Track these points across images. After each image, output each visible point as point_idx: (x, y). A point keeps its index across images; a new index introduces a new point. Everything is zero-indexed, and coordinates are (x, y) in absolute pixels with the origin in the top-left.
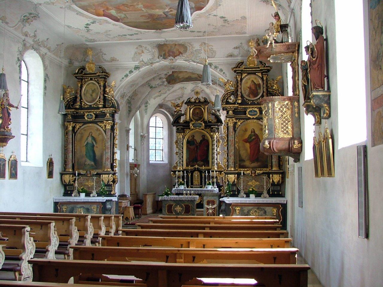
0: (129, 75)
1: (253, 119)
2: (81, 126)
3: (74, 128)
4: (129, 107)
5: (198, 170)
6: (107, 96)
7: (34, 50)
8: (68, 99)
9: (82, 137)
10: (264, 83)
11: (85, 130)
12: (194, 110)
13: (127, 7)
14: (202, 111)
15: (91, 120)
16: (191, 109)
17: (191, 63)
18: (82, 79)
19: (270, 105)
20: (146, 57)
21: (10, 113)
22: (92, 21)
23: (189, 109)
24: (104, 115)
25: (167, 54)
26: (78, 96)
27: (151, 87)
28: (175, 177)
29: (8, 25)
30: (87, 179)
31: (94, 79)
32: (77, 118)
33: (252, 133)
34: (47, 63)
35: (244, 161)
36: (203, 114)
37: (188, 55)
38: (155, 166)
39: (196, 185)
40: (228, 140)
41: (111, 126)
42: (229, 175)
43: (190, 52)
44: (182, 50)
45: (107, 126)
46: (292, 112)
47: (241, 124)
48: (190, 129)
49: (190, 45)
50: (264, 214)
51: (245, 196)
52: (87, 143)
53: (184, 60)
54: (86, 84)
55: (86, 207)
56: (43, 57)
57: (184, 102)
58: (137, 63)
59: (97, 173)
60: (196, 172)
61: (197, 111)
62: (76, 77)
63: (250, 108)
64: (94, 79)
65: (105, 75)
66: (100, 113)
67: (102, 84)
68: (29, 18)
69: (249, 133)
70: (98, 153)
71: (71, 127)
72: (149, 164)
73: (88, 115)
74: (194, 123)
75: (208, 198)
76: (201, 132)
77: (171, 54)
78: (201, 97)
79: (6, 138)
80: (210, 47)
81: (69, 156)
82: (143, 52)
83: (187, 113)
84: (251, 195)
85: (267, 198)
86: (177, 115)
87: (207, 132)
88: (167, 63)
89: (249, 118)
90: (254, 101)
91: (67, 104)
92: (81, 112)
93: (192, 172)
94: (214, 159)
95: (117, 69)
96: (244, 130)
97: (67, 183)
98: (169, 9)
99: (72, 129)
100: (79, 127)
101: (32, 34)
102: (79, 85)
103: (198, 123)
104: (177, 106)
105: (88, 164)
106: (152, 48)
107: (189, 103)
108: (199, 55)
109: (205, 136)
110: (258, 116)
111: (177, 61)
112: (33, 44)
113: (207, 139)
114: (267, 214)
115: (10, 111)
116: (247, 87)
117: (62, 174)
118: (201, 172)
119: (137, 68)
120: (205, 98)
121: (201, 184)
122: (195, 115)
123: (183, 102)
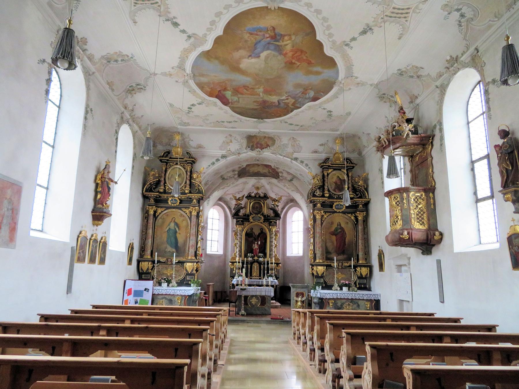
0: (216, 163)
1: (339, 212)
2: (163, 210)
3: (155, 212)
6: (194, 182)
7: (129, 125)
8: (151, 182)
9: (163, 223)
10: (349, 179)
11: (167, 215)
12: (254, 204)
13: (246, 90)
14: (261, 205)
15: (175, 205)
17: (278, 156)
18: (167, 163)
19: (405, 195)
20: (234, 147)
21: (110, 188)
22: (200, 101)
23: (249, 203)
24: (190, 200)
25: (255, 146)
26: (162, 179)
29: (114, 92)
30: (166, 267)
31: (180, 164)
32: (158, 201)
33: (338, 226)
34: (136, 142)
35: (330, 253)
36: (262, 209)
37: (275, 148)
38: (211, 256)
39: (255, 277)
40: (314, 233)
41: (197, 212)
42: (318, 267)
43: (278, 146)
44: (270, 143)
45: (193, 212)
46: (427, 203)
47: (327, 217)
48: (249, 221)
49: (279, 139)
50: (358, 308)
51: (339, 289)
52: (169, 229)
53: (271, 153)
54: (171, 169)
55: (168, 299)
56: (134, 134)
58: (224, 152)
59: (179, 261)
60: (256, 263)
61: (257, 205)
62: (161, 160)
63: (336, 202)
64: (180, 164)
65: (193, 161)
66: (185, 199)
67: (189, 170)
68: (133, 90)
69: (335, 226)
70: (181, 240)
71: (152, 211)
72: (207, 255)
73: (172, 200)
74: (254, 217)
75: (297, 290)
77: (259, 146)
78: (261, 192)
79: (104, 215)
80: (297, 142)
81: (148, 242)
82: (231, 142)
83: (248, 207)
84: (344, 288)
85: (339, 291)
88: (254, 154)
89: (336, 212)
90: (340, 196)
91: (149, 187)
92: (164, 196)
93: (252, 263)
94: (272, 252)
95: (203, 156)
96: (331, 223)
97: (145, 271)
98: (286, 97)
99: (154, 213)
100: (161, 212)
101: (131, 108)
102: (164, 169)
104: (238, 199)
105: (168, 250)
106: (241, 138)
107: (249, 197)
108: (286, 149)
110: (344, 210)
111: (264, 153)
112: (129, 119)
114: (361, 307)
115: (110, 186)
116: (333, 182)
117: (139, 262)
118: (260, 263)
119: (224, 157)
121: (260, 276)
123: (243, 196)
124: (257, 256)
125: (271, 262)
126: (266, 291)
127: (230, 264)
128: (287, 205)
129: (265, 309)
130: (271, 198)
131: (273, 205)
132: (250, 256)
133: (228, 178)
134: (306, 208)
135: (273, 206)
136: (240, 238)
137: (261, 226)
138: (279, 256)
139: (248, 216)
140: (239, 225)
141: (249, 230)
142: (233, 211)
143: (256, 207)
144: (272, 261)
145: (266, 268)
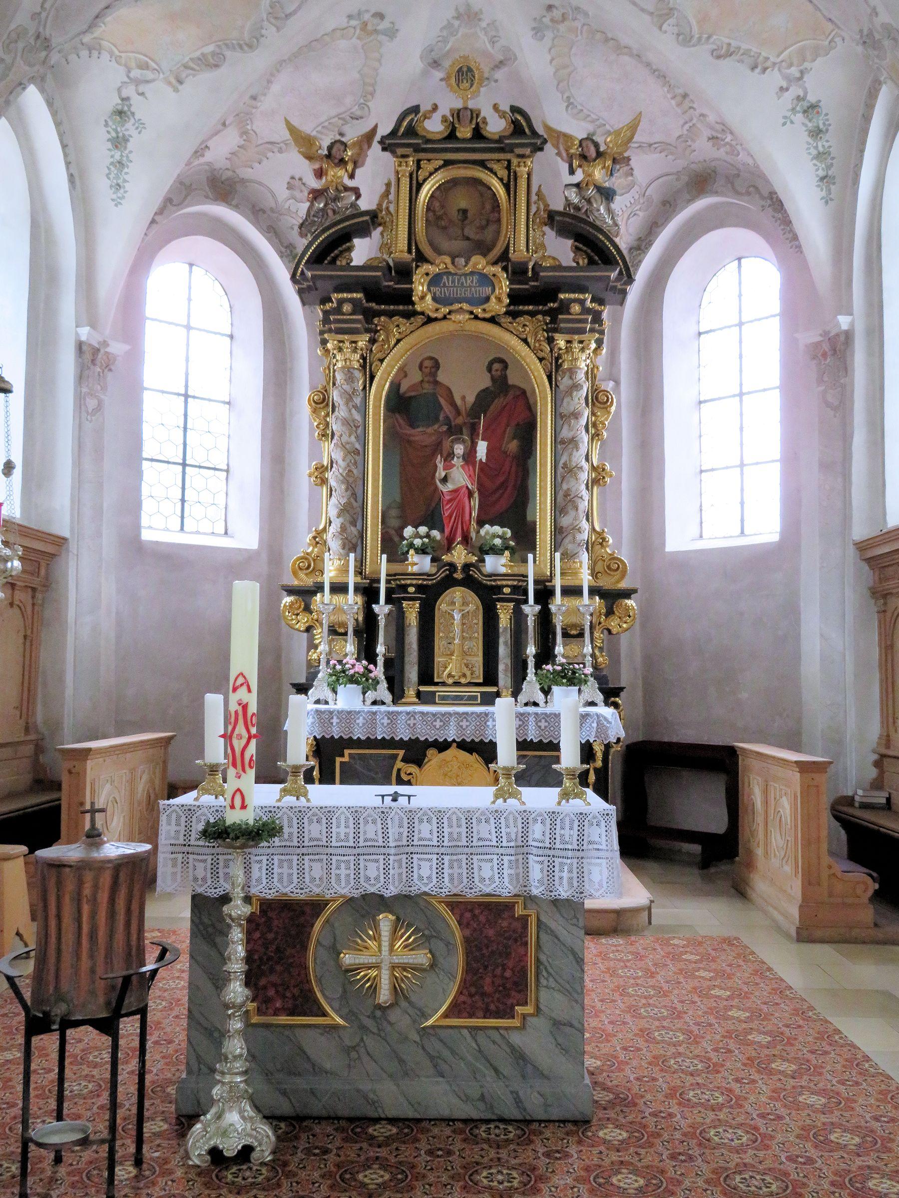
5: (470, 581)
12: (444, 189)
16: (419, 186)
28: (308, 629)
39: (457, 684)
57: (378, 138)
60: (458, 593)
61: (461, 200)
76: (478, 338)
86: (332, 218)
87: (525, 341)
94: (572, 513)
103: (468, 269)
104: (329, 156)
109: (506, 366)
113: (522, 386)
120: (515, 109)
121: (490, 678)
122: (445, 228)
123: (369, 137)
124: (466, 540)
125: (571, 582)
126: (522, 848)
127: (288, 600)
128: (667, 220)
129: (519, 1057)
131: (577, 185)
132: (418, 542)
135: (576, 200)
136: (346, 422)
137: (499, 347)
138: (618, 544)
140: (339, 331)
141: (416, 376)
142: (301, 243)
143: (454, 214)
144: (576, 573)
145: (531, 622)
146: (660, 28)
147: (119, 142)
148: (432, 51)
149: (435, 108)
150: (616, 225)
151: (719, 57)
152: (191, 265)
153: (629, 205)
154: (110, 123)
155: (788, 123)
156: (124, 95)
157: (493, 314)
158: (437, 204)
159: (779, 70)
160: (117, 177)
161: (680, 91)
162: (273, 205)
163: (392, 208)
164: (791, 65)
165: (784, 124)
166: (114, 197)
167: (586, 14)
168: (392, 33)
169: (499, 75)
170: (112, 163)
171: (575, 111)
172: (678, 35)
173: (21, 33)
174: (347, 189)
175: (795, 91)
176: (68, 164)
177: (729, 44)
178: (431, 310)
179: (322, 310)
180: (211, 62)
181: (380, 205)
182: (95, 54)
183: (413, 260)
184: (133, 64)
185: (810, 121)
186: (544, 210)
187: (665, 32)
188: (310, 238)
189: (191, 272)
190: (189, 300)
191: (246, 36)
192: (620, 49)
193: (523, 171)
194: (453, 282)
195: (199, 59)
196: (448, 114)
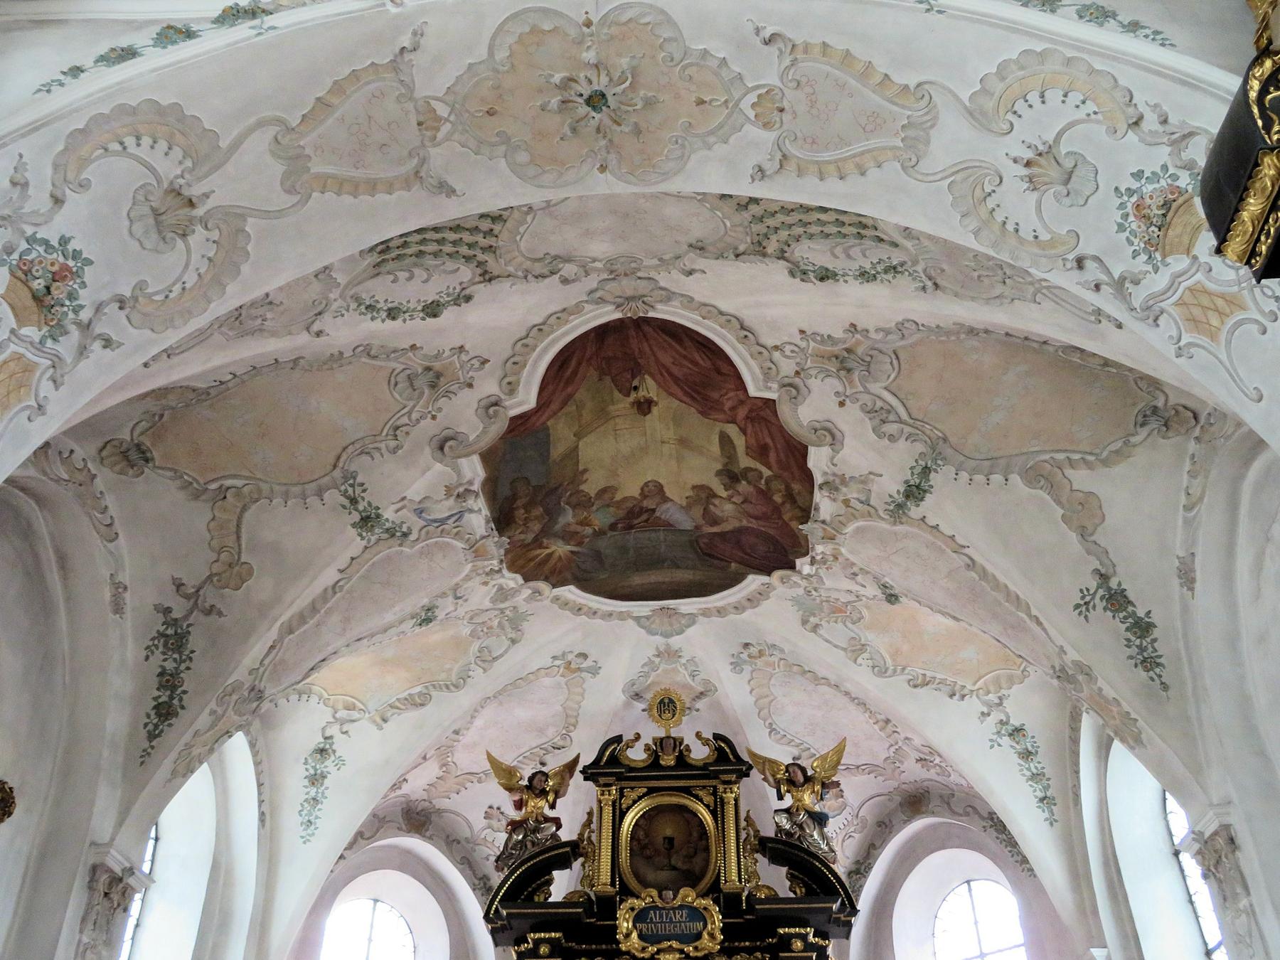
4: (161, 675)
12: (646, 817)
14: (701, 824)
16: (623, 814)
27: (368, 521)
36: (707, 849)
57: (580, 767)
86: (531, 850)
103: (677, 902)
104: (529, 787)
120: (717, 737)
122: (649, 858)
123: (570, 767)
128: (884, 842)
130: (767, 765)
131: (787, 811)
133: (416, 523)
134: (1041, 815)
135: (787, 826)
139: (607, 906)
142: (496, 878)
143: (660, 840)
146: (855, 661)
147: (316, 779)
148: (633, 685)
149: (638, 737)
150: (833, 851)
151: (915, 686)
152: (376, 901)
153: (842, 827)
154: (310, 761)
155: (996, 745)
156: (328, 734)
157: (706, 952)
158: (641, 834)
159: (977, 696)
160: (310, 814)
161: (883, 717)
162: (468, 834)
163: (594, 837)
164: (988, 692)
165: (992, 747)
166: (304, 834)
167: (782, 651)
168: (594, 671)
169: (700, 704)
170: (306, 800)
171: (779, 736)
172: (873, 667)
173: (237, 687)
174: (547, 819)
175: (996, 716)
176: (261, 802)
177: (924, 675)
178: (637, 949)
179: (516, 952)
180: (417, 702)
181: (581, 835)
182: (305, 697)
183: (617, 893)
184: (340, 706)
185: (1018, 743)
186: (755, 837)
187: (861, 665)
188: (506, 872)
189: (374, 909)
190: (370, 940)
191: (454, 678)
192: (818, 680)
193: (730, 797)
194: (661, 916)
195: (406, 699)
196: (651, 743)
